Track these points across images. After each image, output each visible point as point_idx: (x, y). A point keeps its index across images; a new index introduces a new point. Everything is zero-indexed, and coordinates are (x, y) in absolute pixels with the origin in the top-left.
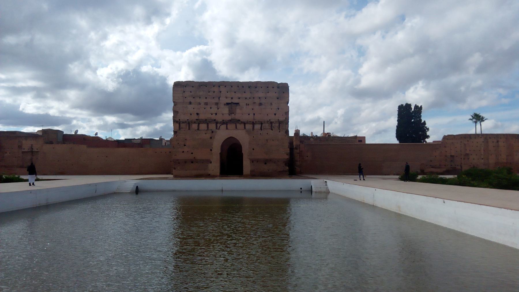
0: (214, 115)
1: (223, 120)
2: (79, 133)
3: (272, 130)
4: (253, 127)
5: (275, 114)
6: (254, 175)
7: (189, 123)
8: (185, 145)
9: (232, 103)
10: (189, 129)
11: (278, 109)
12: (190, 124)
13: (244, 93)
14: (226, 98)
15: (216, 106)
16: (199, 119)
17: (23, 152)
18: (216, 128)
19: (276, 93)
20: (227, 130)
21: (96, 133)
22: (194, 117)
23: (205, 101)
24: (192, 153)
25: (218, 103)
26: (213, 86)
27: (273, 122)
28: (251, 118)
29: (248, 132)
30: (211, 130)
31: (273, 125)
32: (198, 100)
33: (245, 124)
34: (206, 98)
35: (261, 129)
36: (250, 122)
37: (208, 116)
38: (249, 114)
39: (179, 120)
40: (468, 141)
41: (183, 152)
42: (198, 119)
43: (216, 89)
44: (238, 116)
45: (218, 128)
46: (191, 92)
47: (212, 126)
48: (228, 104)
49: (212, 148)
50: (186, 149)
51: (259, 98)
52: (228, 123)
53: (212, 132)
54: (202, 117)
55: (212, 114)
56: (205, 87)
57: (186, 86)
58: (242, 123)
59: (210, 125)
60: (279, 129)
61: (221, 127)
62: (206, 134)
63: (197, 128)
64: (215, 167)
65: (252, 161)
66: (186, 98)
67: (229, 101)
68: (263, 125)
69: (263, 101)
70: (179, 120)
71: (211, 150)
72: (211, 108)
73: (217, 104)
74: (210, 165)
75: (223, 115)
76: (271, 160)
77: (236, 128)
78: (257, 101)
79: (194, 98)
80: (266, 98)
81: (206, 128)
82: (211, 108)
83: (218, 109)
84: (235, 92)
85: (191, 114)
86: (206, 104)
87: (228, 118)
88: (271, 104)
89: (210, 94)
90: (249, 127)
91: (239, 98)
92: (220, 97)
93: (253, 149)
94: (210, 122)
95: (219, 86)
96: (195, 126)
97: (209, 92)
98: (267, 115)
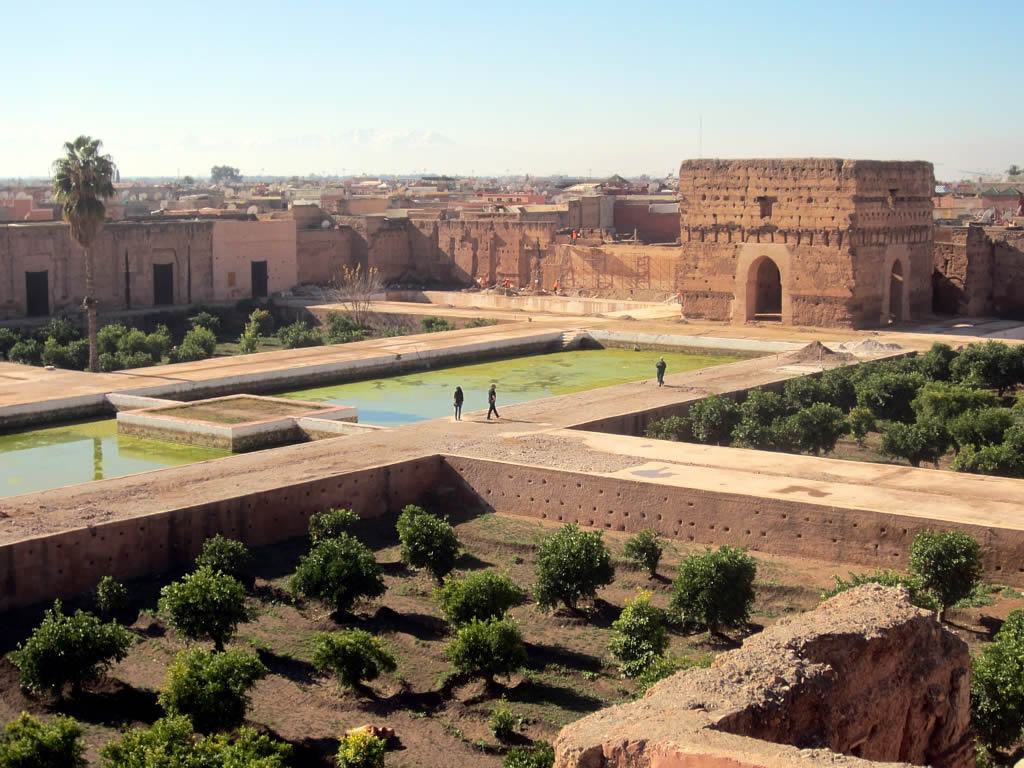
5: (833, 218)
7: (703, 232)
15: (742, 203)
22: (710, 221)
23: (724, 192)
28: (793, 223)
29: (792, 250)
32: (717, 193)
37: (730, 219)
41: (694, 278)
43: (741, 173)
48: (760, 199)
50: (697, 274)
51: (809, 189)
54: (721, 220)
58: (780, 232)
63: (714, 240)
64: (738, 305)
65: (795, 298)
69: (814, 194)
71: (734, 277)
72: (734, 205)
73: (743, 199)
75: (752, 217)
78: (805, 194)
82: (734, 205)
86: (726, 198)
87: (760, 223)
88: (827, 200)
89: (732, 181)
90: (792, 240)
94: (733, 229)
96: (711, 236)
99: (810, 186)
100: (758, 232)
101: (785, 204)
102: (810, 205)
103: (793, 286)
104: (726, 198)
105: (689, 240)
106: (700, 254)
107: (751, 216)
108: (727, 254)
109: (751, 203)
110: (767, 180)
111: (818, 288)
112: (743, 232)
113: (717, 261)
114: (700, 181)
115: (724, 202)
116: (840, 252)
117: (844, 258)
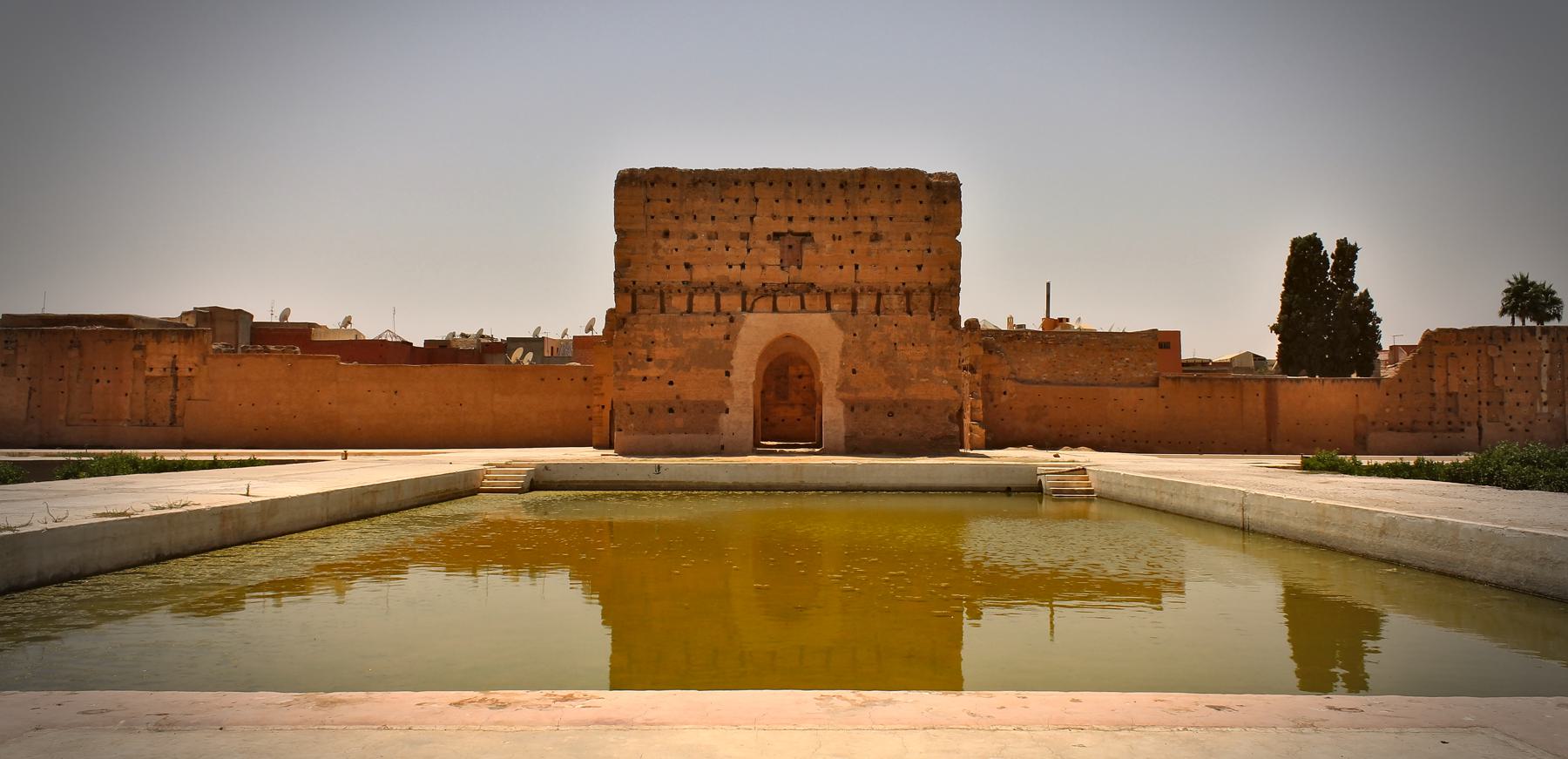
0: (737, 268)
1: (764, 285)
2: (291, 320)
3: (910, 313)
4: (855, 305)
6: (853, 446)
8: (649, 360)
9: (790, 232)
10: (663, 311)
11: (929, 251)
12: (666, 296)
13: (825, 205)
14: (774, 217)
16: (691, 282)
17: (148, 380)
18: (744, 309)
19: (921, 202)
20: (775, 315)
21: (346, 318)
23: (710, 226)
24: (671, 383)
25: (748, 234)
26: (733, 184)
27: (914, 291)
28: (846, 277)
29: (841, 324)
30: (728, 314)
31: (914, 298)
33: (828, 295)
34: (713, 218)
35: (878, 312)
36: (844, 290)
38: (841, 267)
39: (634, 283)
40: (1500, 348)
42: (688, 280)
43: (744, 192)
44: (805, 275)
45: (748, 307)
46: (668, 201)
47: (731, 302)
48: (777, 235)
49: (732, 367)
50: (653, 371)
51: (872, 218)
52: (777, 293)
53: (732, 320)
54: (701, 274)
55: (730, 267)
56: (711, 185)
57: (652, 184)
59: (724, 300)
60: (931, 311)
61: (756, 304)
62: (712, 325)
63: (685, 308)
65: (851, 407)
66: (652, 217)
67: (782, 226)
68: (885, 298)
69: (883, 227)
70: (634, 283)
71: (728, 374)
73: (745, 237)
74: (724, 418)
75: (763, 268)
76: (906, 405)
77: (803, 307)
78: (866, 227)
79: (677, 218)
80: (891, 219)
81: (713, 309)
83: (749, 251)
84: (800, 201)
85: (668, 267)
87: (777, 276)
89: (721, 205)
91: (813, 219)
92: (754, 216)
93: (854, 372)
94: (725, 289)
95: (753, 184)
96: (679, 302)
97: (722, 200)
98: (896, 268)
99: (874, 212)
100: (771, 294)
101: (829, 245)
102: (875, 246)
103: (844, 386)
104: (713, 236)
105: (634, 311)
106: (659, 335)
107: (767, 266)
108: (713, 333)
109: (762, 243)
110: (794, 205)
111: (894, 387)
112: (744, 294)
113: (695, 346)
114: (658, 206)
115: (706, 242)
116: (933, 324)
117: (943, 334)
